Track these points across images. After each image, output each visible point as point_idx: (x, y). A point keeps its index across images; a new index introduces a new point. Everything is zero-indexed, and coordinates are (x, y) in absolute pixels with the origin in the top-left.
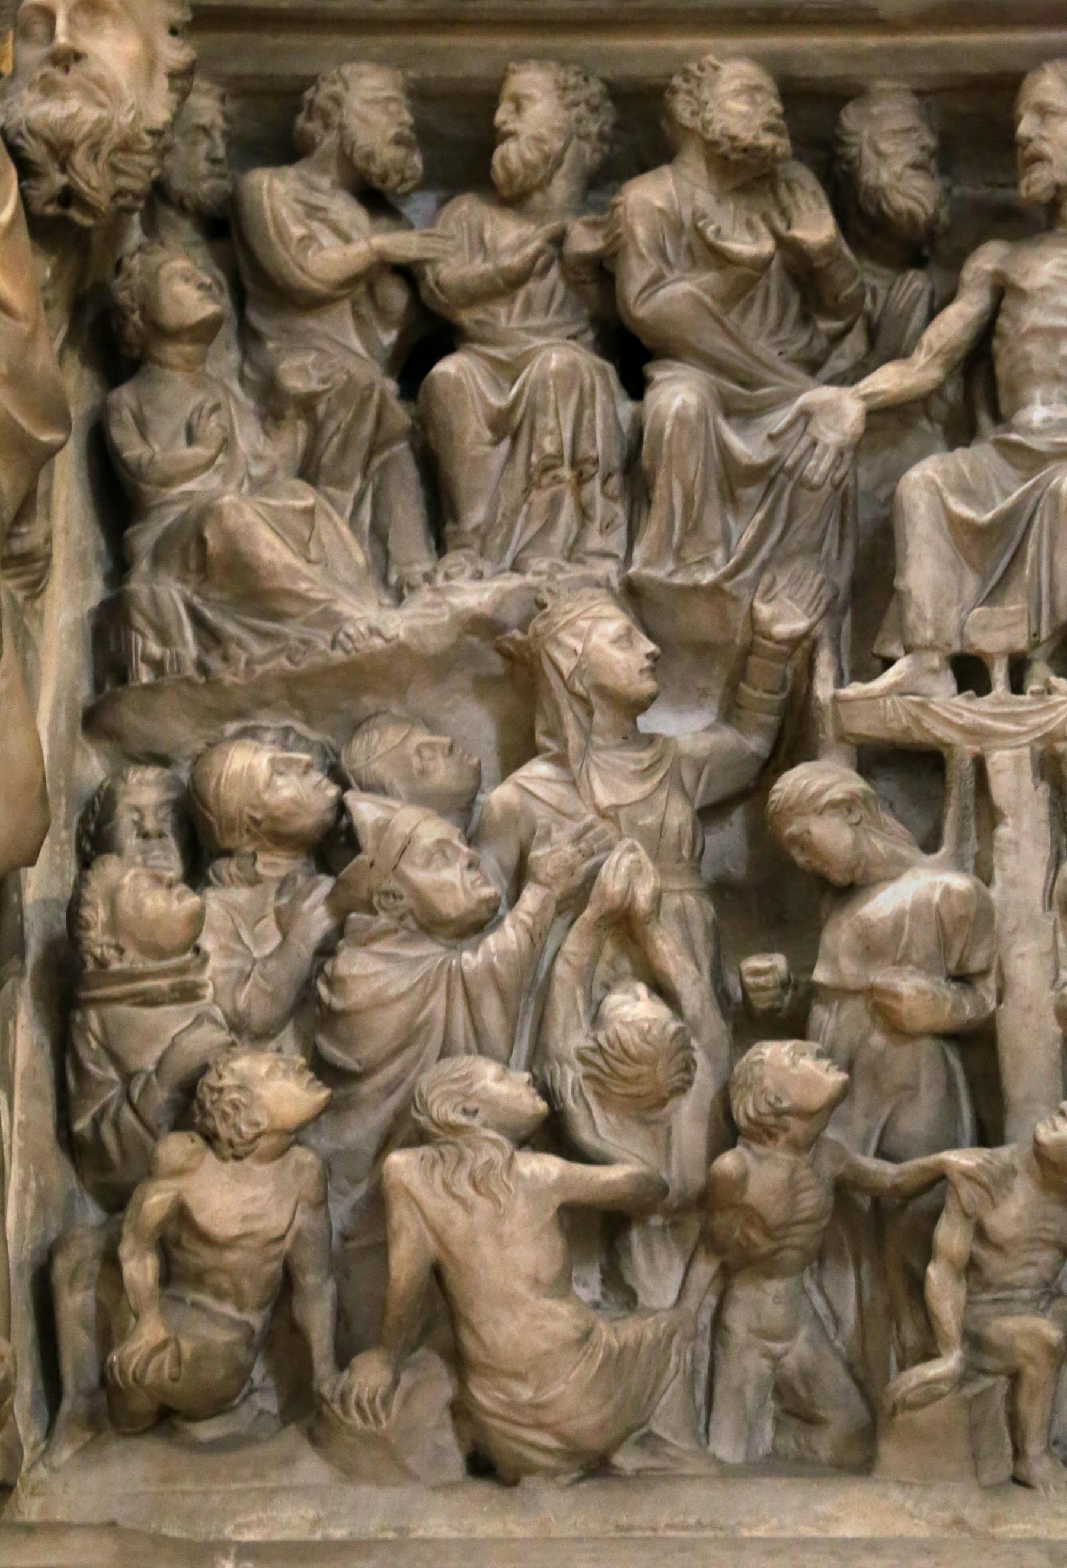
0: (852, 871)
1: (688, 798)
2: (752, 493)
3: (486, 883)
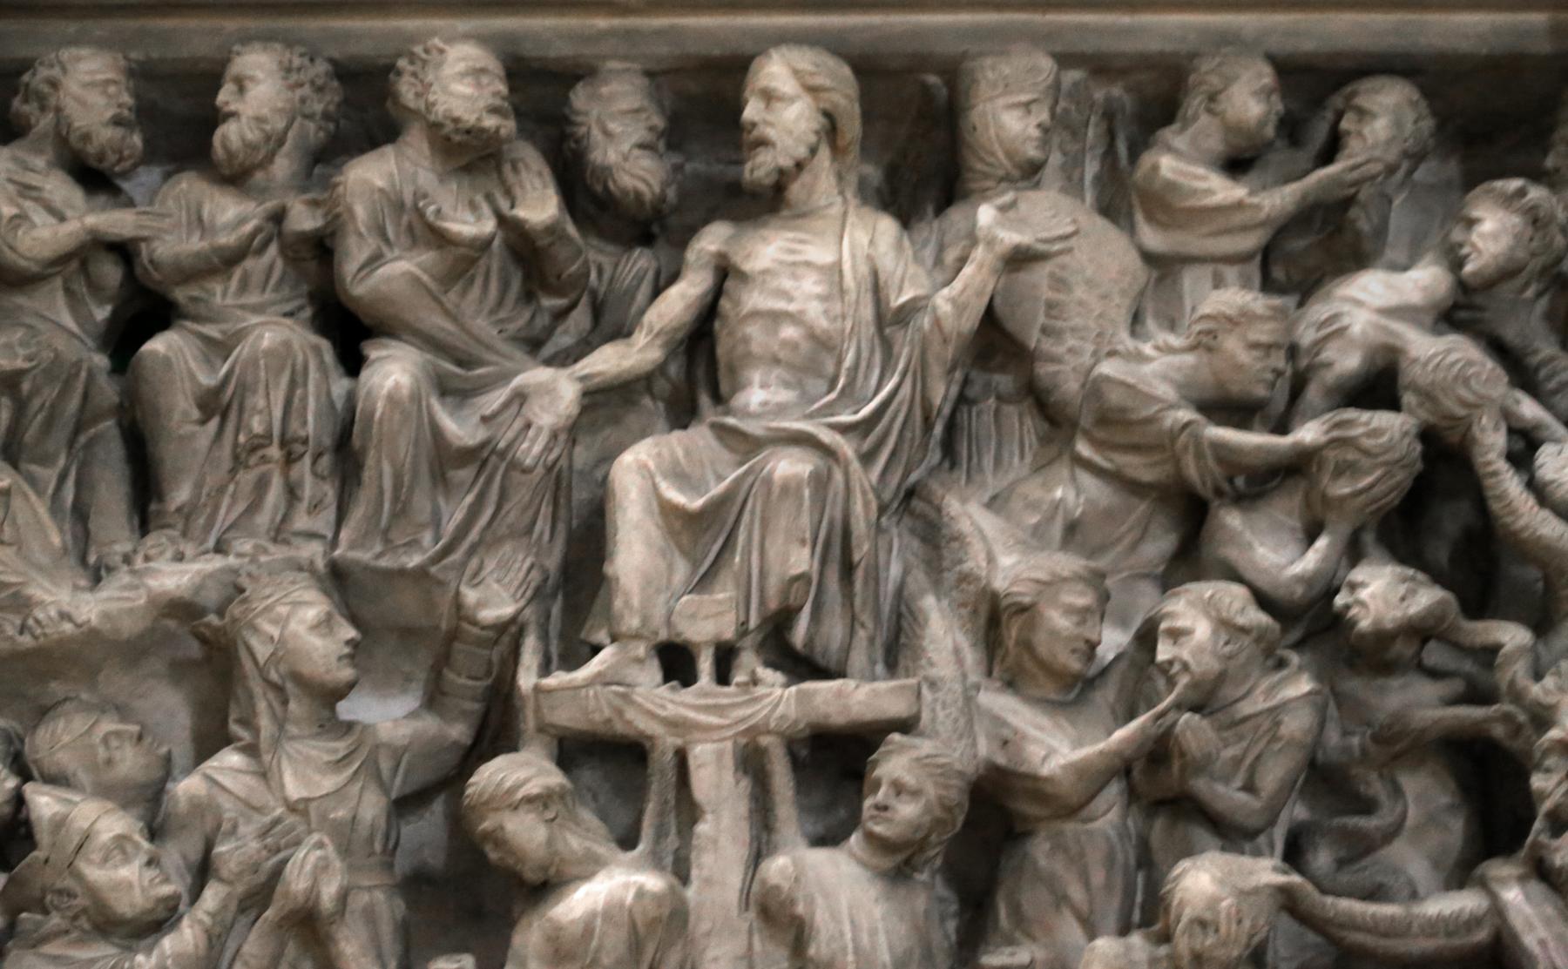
0: (545, 869)
1: (384, 788)
2: (464, 474)
3: (166, 880)
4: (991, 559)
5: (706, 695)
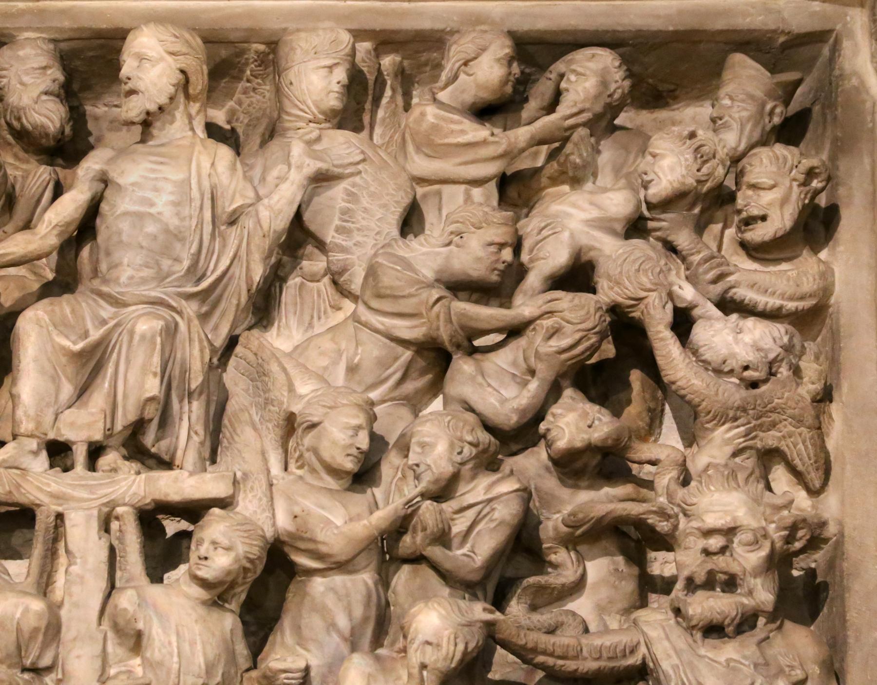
4: (291, 389)
5: (81, 478)
